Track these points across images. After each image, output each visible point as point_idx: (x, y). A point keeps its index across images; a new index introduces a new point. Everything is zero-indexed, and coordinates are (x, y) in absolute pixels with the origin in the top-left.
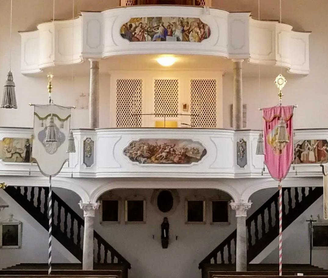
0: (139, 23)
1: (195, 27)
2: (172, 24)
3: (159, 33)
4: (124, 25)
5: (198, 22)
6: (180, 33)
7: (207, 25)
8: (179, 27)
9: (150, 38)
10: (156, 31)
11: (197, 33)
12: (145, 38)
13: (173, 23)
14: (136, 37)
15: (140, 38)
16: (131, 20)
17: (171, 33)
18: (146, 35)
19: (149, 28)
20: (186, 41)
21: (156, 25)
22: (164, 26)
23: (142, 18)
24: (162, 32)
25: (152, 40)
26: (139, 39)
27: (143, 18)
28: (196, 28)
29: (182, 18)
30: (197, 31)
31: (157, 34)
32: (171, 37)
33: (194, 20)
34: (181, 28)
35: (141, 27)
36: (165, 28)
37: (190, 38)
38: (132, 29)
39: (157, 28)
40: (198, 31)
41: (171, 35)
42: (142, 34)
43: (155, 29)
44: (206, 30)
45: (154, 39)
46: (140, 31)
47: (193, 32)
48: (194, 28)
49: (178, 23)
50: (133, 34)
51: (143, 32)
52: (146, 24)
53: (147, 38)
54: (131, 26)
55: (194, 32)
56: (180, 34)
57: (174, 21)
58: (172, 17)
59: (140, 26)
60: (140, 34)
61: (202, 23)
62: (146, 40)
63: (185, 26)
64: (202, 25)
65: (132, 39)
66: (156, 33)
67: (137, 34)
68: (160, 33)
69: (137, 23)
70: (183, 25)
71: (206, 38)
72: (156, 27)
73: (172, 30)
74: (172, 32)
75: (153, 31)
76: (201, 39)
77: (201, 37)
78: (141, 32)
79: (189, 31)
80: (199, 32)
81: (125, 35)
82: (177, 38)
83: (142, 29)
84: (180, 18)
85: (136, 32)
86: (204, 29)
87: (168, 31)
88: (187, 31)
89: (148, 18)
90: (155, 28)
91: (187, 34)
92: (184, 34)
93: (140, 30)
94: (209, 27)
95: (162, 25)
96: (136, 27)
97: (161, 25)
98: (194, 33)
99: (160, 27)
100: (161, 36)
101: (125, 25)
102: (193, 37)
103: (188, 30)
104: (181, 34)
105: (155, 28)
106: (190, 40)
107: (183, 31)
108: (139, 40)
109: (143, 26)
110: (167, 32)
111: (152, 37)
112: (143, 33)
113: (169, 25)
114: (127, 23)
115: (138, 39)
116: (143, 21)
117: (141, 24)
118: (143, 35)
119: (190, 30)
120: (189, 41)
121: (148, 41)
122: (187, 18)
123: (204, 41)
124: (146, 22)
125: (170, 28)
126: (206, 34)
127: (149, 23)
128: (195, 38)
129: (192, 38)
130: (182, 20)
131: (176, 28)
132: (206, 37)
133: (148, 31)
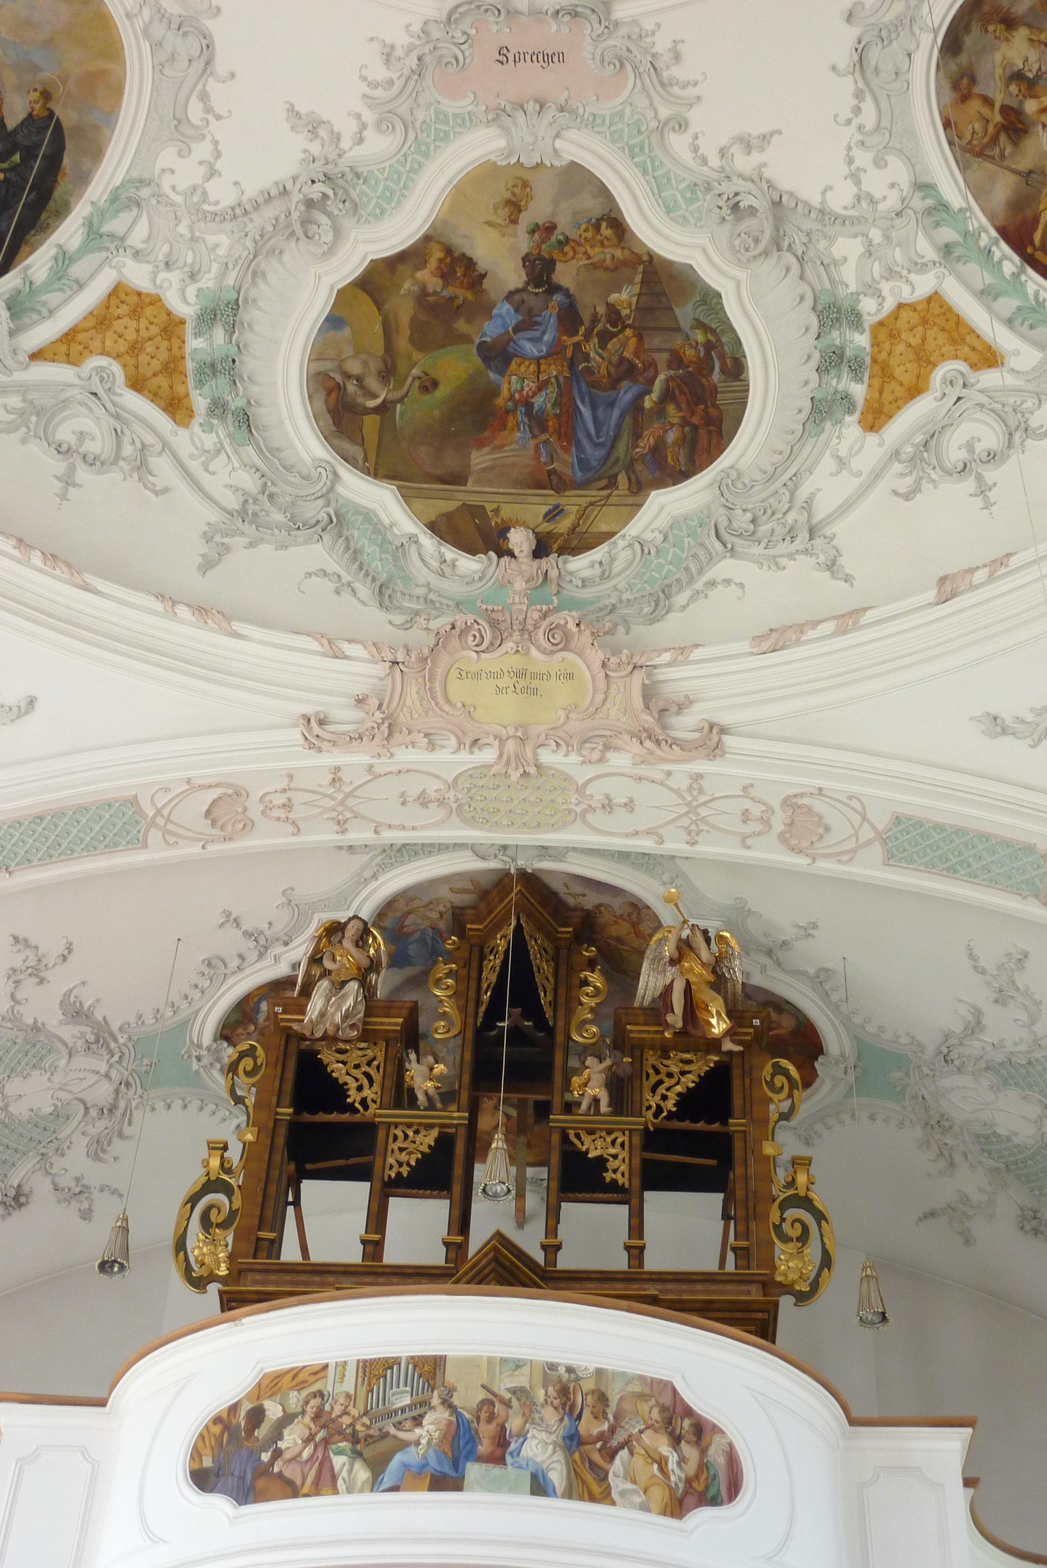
0: (305, 1393)
1: (647, 1428)
2: (507, 1396)
3: (424, 1441)
4: (217, 1420)
5: (666, 1400)
6: (551, 1448)
7: (716, 1429)
8: (551, 1416)
9: (362, 1474)
10: (402, 1435)
11: (662, 1463)
12: (334, 1478)
13: (514, 1391)
14: (280, 1475)
15: (304, 1478)
16: (259, 1385)
17: (499, 1445)
18: (339, 1462)
19: (366, 1420)
20: (593, 1499)
21: (406, 1400)
22: (452, 1407)
23: (326, 1367)
24: (444, 1437)
25: (374, 1484)
26: (299, 1482)
27: (331, 1371)
28: (649, 1432)
29: (570, 1370)
30: (656, 1450)
31: (412, 1449)
32: (496, 1471)
33: (637, 1388)
34: (562, 1420)
35: (317, 1417)
36: (459, 1416)
37: (617, 1483)
38: (261, 1433)
39: (414, 1419)
40: (665, 1449)
41: (497, 1458)
42: (320, 1454)
43: (398, 1425)
44: (716, 1456)
45: (388, 1480)
46: (307, 1441)
47: (632, 1453)
48: (641, 1432)
49: (540, 1395)
50: (265, 1457)
51: (326, 1442)
52: (348, 1396)
53: (344, 1473)
54: (257, 1415)
55: (638, 1450)
56: (554, 1452)
57: (521, 1380)
58: (504, 1361)
59: (310, 1411)
60: (306, 1454)
61: (689, 1412)
62: (340, 1482)
63: (587, 1415)
64: (687, 1423)
65: (252, 1487)
66: (404, 1445)
67: (287, 1455)
68: (429, 1442)
69: (294, 1400)
70: (572, 1407)
71: (714, 1501)
72: (403, 1410)
73: (503, 1428)
74: (502, 1441)
75: (385, 1435)
76: (681, 1502)
77: (686, 1493)
78: (312, 1446)
79: (605, 1443)
80: (673, 1458)
81: (217, 1475)
82: (534, 1477)
83: (324, 1426)
84: (553, 1367)
85: (281, 1445)
86: (703, 1452)
87: (477, 1431)
88: (599, 1445)
89: (365, 1361)
90: (400, 1417)
91: (597, 1457)
92: (577, 1456)
93: (306, 1433)
94: (731, 1445)
95: (447, 1403)
96: (288, 1419)
97: (435, 1401)
98: (639, 1462)
99: (431, 1408)
100: (433, 1463)
101: (225, 1416)
102: (634, 1482)
103: (601, 1437)
104: (559, 1456)
105: (400, 1417)
106: (614, 1495)
107: (573, 1441)
108: (291, 1490)
109: (327, 1408)
110: (473, 1440)
111: (377, 1466)
112: (326, 1449)
113: (484, 1402)
114: (234, 1408)
115: (290, 1483)
116: (328, 1385)
117: (314, 1402)
118: (326, 1462)
119: (614, 1443)
120: (605, 1497)
121: (349, 1491)
122: (600, 1373)
123: (702, 1517)
124: (349, 1386)
125: (491, 1418)
126: (715, 1477)
127: (362, 1390)
128: (645, 1491)
129: (630, 1486)
130: (569, 1380)
131: (528, 1418)
132: (710, 1494)
133: (354, 1439)
